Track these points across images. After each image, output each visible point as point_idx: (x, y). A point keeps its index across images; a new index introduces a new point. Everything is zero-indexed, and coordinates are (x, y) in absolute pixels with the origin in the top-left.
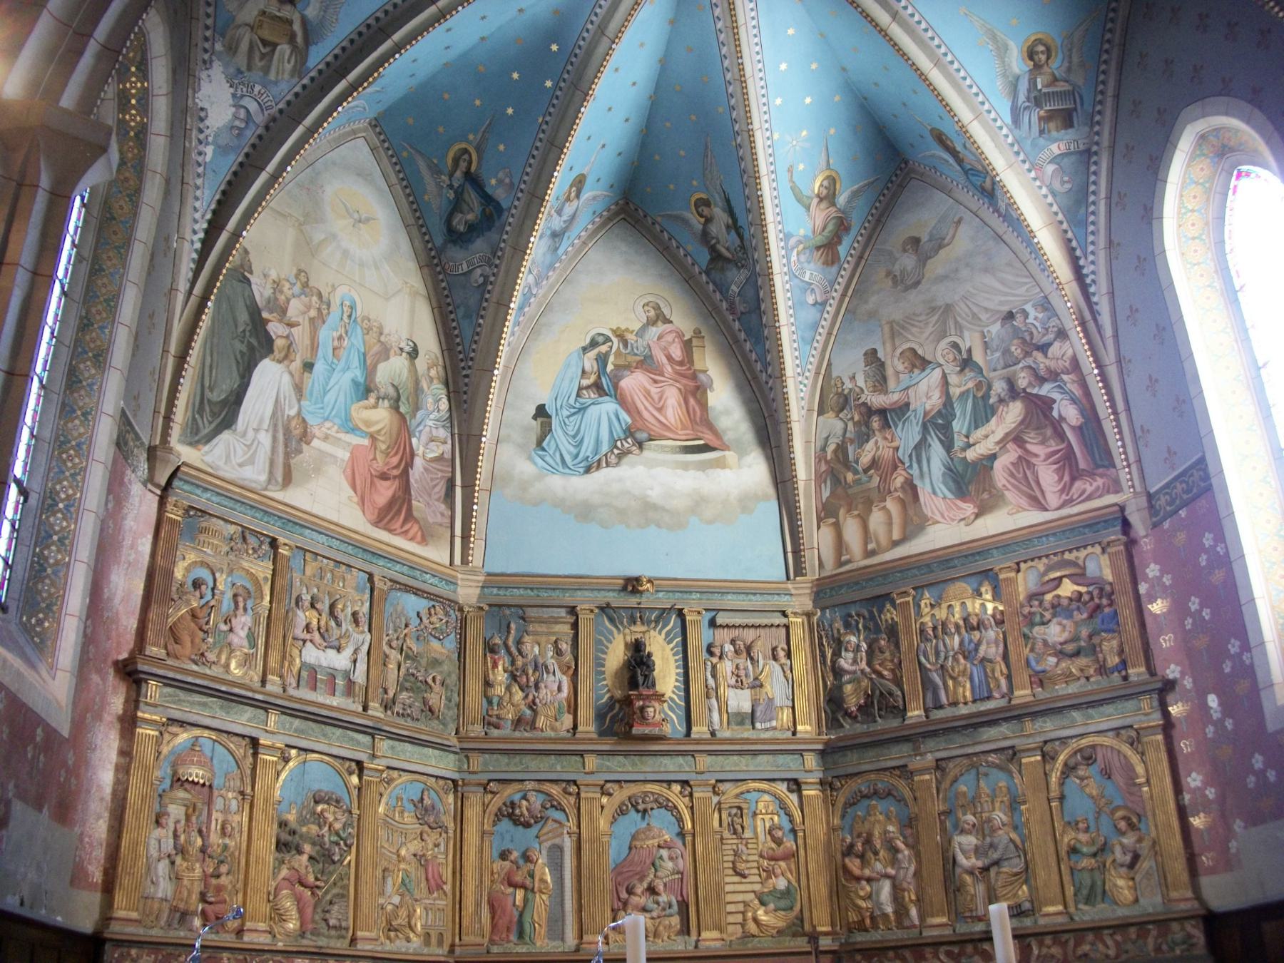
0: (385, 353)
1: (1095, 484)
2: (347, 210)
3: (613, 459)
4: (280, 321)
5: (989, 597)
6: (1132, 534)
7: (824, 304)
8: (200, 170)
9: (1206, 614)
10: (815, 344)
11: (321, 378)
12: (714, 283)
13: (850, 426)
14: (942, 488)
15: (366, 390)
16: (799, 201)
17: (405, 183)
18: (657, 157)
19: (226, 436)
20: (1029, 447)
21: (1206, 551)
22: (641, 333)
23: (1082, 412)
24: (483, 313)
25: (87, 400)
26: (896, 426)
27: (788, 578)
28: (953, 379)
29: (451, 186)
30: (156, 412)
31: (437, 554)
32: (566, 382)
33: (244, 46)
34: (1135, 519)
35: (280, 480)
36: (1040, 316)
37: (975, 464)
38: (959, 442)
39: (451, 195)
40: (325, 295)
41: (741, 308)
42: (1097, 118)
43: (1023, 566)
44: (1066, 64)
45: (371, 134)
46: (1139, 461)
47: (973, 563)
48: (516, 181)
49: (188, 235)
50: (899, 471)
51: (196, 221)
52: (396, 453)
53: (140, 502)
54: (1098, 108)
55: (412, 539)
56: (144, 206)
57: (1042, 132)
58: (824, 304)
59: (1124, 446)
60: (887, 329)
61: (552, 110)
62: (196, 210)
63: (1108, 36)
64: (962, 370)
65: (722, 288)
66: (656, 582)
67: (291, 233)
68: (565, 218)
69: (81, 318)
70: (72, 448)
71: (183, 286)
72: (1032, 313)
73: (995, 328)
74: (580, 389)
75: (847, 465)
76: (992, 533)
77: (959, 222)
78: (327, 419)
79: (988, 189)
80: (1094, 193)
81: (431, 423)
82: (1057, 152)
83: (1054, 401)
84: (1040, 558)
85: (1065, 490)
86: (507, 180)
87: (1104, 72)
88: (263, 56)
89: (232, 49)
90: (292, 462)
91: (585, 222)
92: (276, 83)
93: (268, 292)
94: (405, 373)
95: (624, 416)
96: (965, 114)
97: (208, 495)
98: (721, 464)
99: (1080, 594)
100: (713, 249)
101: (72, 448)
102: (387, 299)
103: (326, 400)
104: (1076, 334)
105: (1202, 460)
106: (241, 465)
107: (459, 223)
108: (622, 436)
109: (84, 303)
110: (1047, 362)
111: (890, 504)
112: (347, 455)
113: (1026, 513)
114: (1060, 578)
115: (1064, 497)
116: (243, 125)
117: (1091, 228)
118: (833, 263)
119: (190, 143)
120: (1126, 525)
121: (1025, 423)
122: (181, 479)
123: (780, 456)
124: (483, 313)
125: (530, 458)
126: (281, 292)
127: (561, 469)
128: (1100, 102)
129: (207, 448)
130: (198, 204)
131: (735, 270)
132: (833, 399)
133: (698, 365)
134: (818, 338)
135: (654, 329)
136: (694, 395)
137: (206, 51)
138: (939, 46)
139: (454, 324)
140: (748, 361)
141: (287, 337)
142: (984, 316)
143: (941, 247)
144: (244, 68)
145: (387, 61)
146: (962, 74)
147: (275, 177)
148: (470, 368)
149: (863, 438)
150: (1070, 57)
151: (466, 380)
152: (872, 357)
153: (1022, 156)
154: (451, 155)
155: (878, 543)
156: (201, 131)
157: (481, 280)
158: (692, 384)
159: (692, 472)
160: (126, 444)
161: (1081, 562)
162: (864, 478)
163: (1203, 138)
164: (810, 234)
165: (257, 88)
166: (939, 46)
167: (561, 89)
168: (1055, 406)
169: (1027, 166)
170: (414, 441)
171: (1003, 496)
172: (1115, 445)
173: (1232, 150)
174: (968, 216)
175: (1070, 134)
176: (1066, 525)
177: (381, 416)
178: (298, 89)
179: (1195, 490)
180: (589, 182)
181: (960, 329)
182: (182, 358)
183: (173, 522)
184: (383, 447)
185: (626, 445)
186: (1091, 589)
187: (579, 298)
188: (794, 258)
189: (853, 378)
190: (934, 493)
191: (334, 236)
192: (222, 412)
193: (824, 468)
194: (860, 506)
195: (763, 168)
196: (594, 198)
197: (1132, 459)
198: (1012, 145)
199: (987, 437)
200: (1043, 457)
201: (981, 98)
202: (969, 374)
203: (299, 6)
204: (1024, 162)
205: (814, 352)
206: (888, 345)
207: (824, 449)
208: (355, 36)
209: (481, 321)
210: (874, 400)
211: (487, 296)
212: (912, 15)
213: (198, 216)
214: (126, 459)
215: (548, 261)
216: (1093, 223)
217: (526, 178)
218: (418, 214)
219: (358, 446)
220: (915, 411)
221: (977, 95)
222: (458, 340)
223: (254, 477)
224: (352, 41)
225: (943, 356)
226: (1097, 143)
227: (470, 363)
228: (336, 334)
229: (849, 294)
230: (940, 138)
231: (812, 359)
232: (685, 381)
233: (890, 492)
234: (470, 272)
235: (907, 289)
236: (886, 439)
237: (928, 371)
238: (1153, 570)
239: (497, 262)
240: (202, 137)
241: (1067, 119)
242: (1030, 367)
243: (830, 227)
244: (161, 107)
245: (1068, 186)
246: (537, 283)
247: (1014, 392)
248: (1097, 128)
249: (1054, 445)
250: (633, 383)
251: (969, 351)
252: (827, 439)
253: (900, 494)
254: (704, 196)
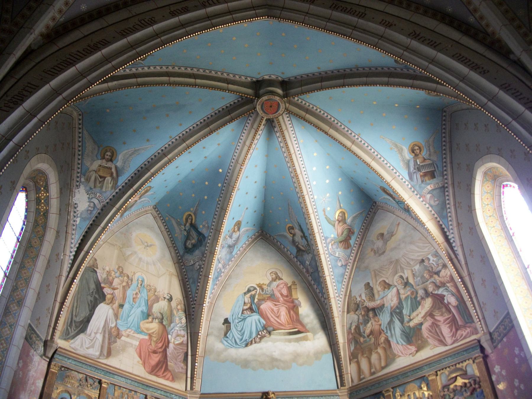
0: (157, 300)
1: (467, 331)
2: (142, 242)
3: (258, 340)
4: (109, 288)
5: (425, 389)
6: (486, 353)
7: (346, 265)
8: (74, 227)
9: (522, 387)
10: (344, 283)
11: (127, 311)
12: (300, 262)
13: (361, 317)
14: (401, 341)
15: (148, 315)
16: (330, 223)
17: (168, 230)
18: (271, 211)
19: (82, 336)
20: (436, 318)
21: (516, 356)
22: (269, 285)
23: (457, 299)
24: (199, 281)
25: (12, 320)
26: (380, 315)
27: (338, 388)
28: (402, 291)
29: (185, 230)
30: (49, 326)
31: (179, 386)
32: (237, 309)
33: (93, 178)
34: (485, 345)
35: (105, 354)
36: (435, 259)
37: (414, 328)
38: (406, 319)
39: (186, 233)
40: (130, 276)
41: (311, 270)
42: (445, 173)
43: (439, 373)
44: (428, 153)
45: (154, 212)
46: (484, 318)
47: (416, 374)
48: (210, 225)
49: (68, 253)
50: (382, 335)
51: (72, 248)
52: (161, 342)
53: (39, 364)
54: (445, 168)
55: (168, 379)
56: (45, 242)
57: (422, 181)
58: (346, 265)
59: (476, 312)
60: (373, 273)
61: (222, 195)
62: (72, 243)
63: (444, 139)
64: (405, 287)
65: (303, 263)
66: (276, 394)
67: (116, 252)
68: (234, 239)
69: (13, 287)
70: (3, 340)
71: (65, 274)
73: (417, 267)
74: (243, 310)
75: (360, 334)
76: (424, 358)
77: (399, 224)
78: (129, 328)
79: (407, 210)
80: (449, 204)
81: (177, 329)
82: (430, 189)
83: (445, 296)
84: (446, 368)
85: (454, 335)
86: (206, 225)
87: (445, 154)
88: (100, 182)
89: (88, 180)
90: (111, 346)
91: (244, 241)
92: (105, 192)
93: (104, 276)
94: (166, 308)
95: (263, 321)
96: (388, 177)
97: (70, 361)
98: (305, 339)
99: (465, 384)
100: (297, 247)
101: (3, 340)
102: (159, 277)
103: (129, 319)
104: (449, 265)
105: (508, 314)
106: (87, 348)
107: (189, 244)
108: (261, 329)
109: (15, 280)
110: (440, 279)
111: (380, 350)
112: (137, 343)
113: (437, 348)
114: (456, 377)
115: (454, 338)
116: (92, 209)
117: (450, 219)
118: (348, 248)
119: (70, 217)
120: (482, 349)
121: (434, 307)
122: (58, 354)
123: (332, 334)
124: (199, 281)
125: (221, 342)
126: (111, 276)
127: (235, 346)
128: (445, 166)
129: (72, 341)
130: (73, 241)
131: (307, 255)
132: (353, 306)
133: (294, 297)
134: (345, 280)
135: (275, 283)
136: (293, 309)
137: (78, 181)
138: (374, 152)
139: (188, 286)
140: (315, 293)
141: (112, 294)
142: (412, 263)
143: (392, 236)
144: (93, 187)
145: (149, 180)
146: (385, 162)
147: (104, 229)
148: (195, 304)
149: (366, 322)
150: (429, 149)
151: (194, 310)
152: (368, 286)
153: (416, 193)
154: (185, 217)
155: (376, 369)
156: (75, 212)
157: (198, 267)
158: (292, 305)
159: (292, 343)
160: (31, 338)
161: (464, 368)
162: (368, 340)
163: (485, 174)
164: (337, 237)
165: (98, 194)
166: (374, 152)
167: (224, 187)
168: (445, 298)
169: (418, 196)
170: (170, 336)
171: (427, 341)
172: (473, 312)
173: (498, 176)
174: (402, 221)
175: (435, 181)
176: (455, 351)
177: (154, 326)
178: (114, 194)
179: (508, 328)
180: (243, 224)
181: (402, 270)
182: (62, 303)
183: (53, 373)
184: (155, 339)
185: (263, 333)
186: (470, 380)
187: (240, 271)
188: (330, 247)
189: (360, 296)
190: (398, 343)
191: (135, 253)
192: (81, 326)
193: (351, 336)
194: (367, 352)
195: (310, 211)
196: (247, 230)
197: (481, 317)
198: (411, 188)
199: (418, 315)
200: (442, 321)
201: (395, 171)
202: (408, 288)
203: (114, 162)
204: (417, 195)
205: (343, 287)
206: (374, 280)
207: (350, 328)
208: (136, 172)
209: (199, 284)
210: (369, 304)
211: (201, 273)
212: (361, 141)
213: (72, 246)
214: (31, 345)
215: (228, 258)
216: (450, 216)
217: (214, 224)
218: (173, 242)
219: (143, 339)
220: (387, 307)
221: (393, 170)
222: (190, 293)
223: (94, 353)
224: (135, 174)
225: (397, 282)
226: (447, 183)
227: (195, 302)
228: (134, 292)
229: (357, 260)
230: (384, 190)
231: (343, 290)
232: (289, 304)
233: (379, 345)
234: (194, 264)
235: (380, 255)
236: (376, 321)
237: (391, 289)
238: (497, 369)
239: (204, 259)
240: (75, 215)
241: (432, 175)
242: (433, 282)
243: (345, 233)
244: (54, 204)
246: (224, 267)
247: (427, 294)
248: (445, 177)
249: (447, 316)
250: (266, 306)
251: (407, 278)
252: (351, 324)
253: (383, 345)
254: (291, 225)
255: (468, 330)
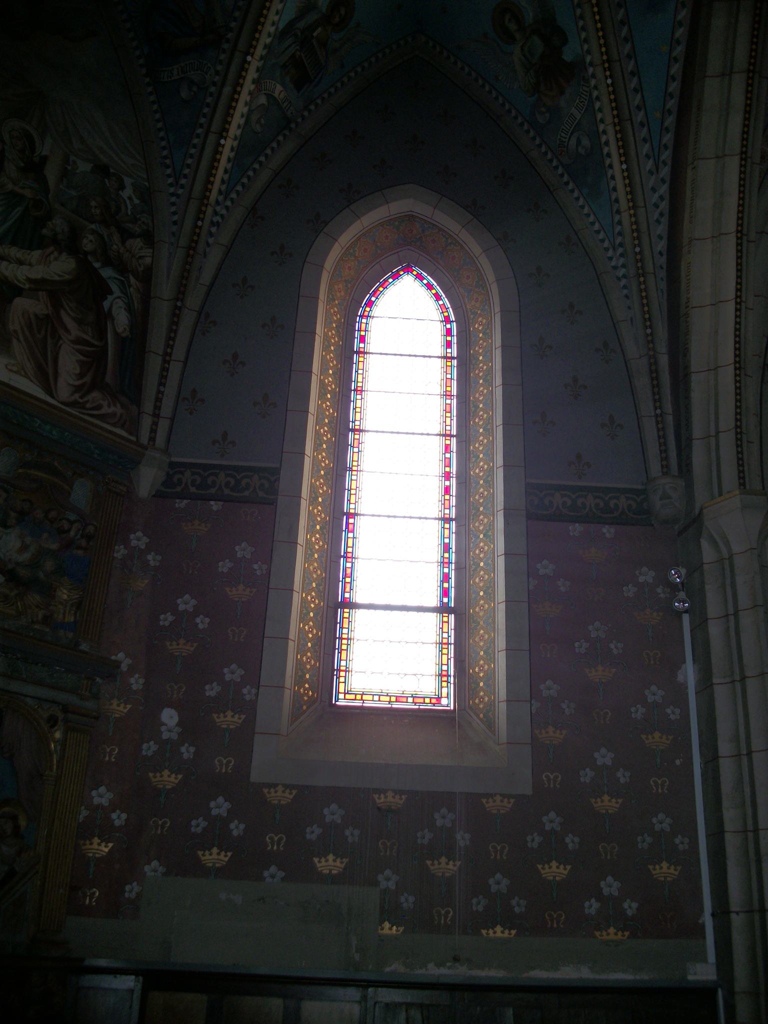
1: (112, 409)
20: (63, 313)
36: (136, 201)
72: (127, 193)
73: (84, 167)
82: (276, 95)
83: (111, 293)
245: (258, 128)
251: (44, 159)
255: (118, 409)
